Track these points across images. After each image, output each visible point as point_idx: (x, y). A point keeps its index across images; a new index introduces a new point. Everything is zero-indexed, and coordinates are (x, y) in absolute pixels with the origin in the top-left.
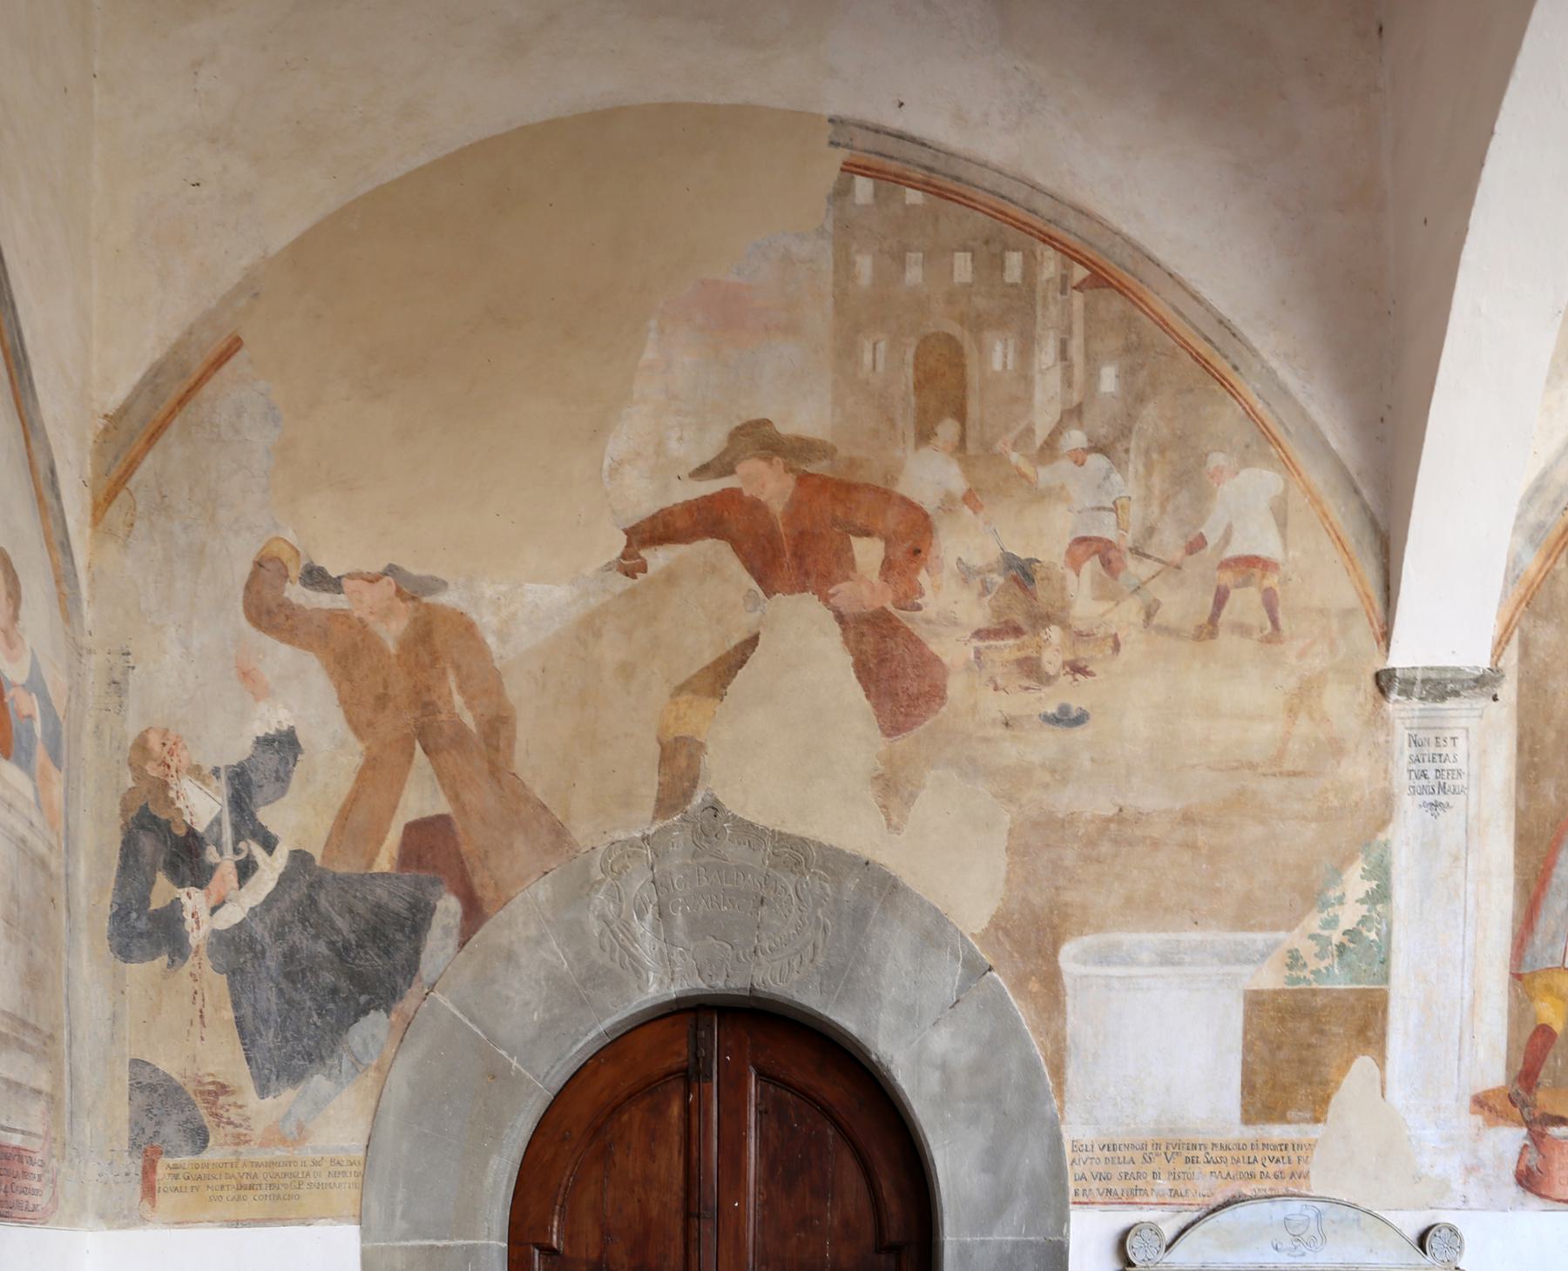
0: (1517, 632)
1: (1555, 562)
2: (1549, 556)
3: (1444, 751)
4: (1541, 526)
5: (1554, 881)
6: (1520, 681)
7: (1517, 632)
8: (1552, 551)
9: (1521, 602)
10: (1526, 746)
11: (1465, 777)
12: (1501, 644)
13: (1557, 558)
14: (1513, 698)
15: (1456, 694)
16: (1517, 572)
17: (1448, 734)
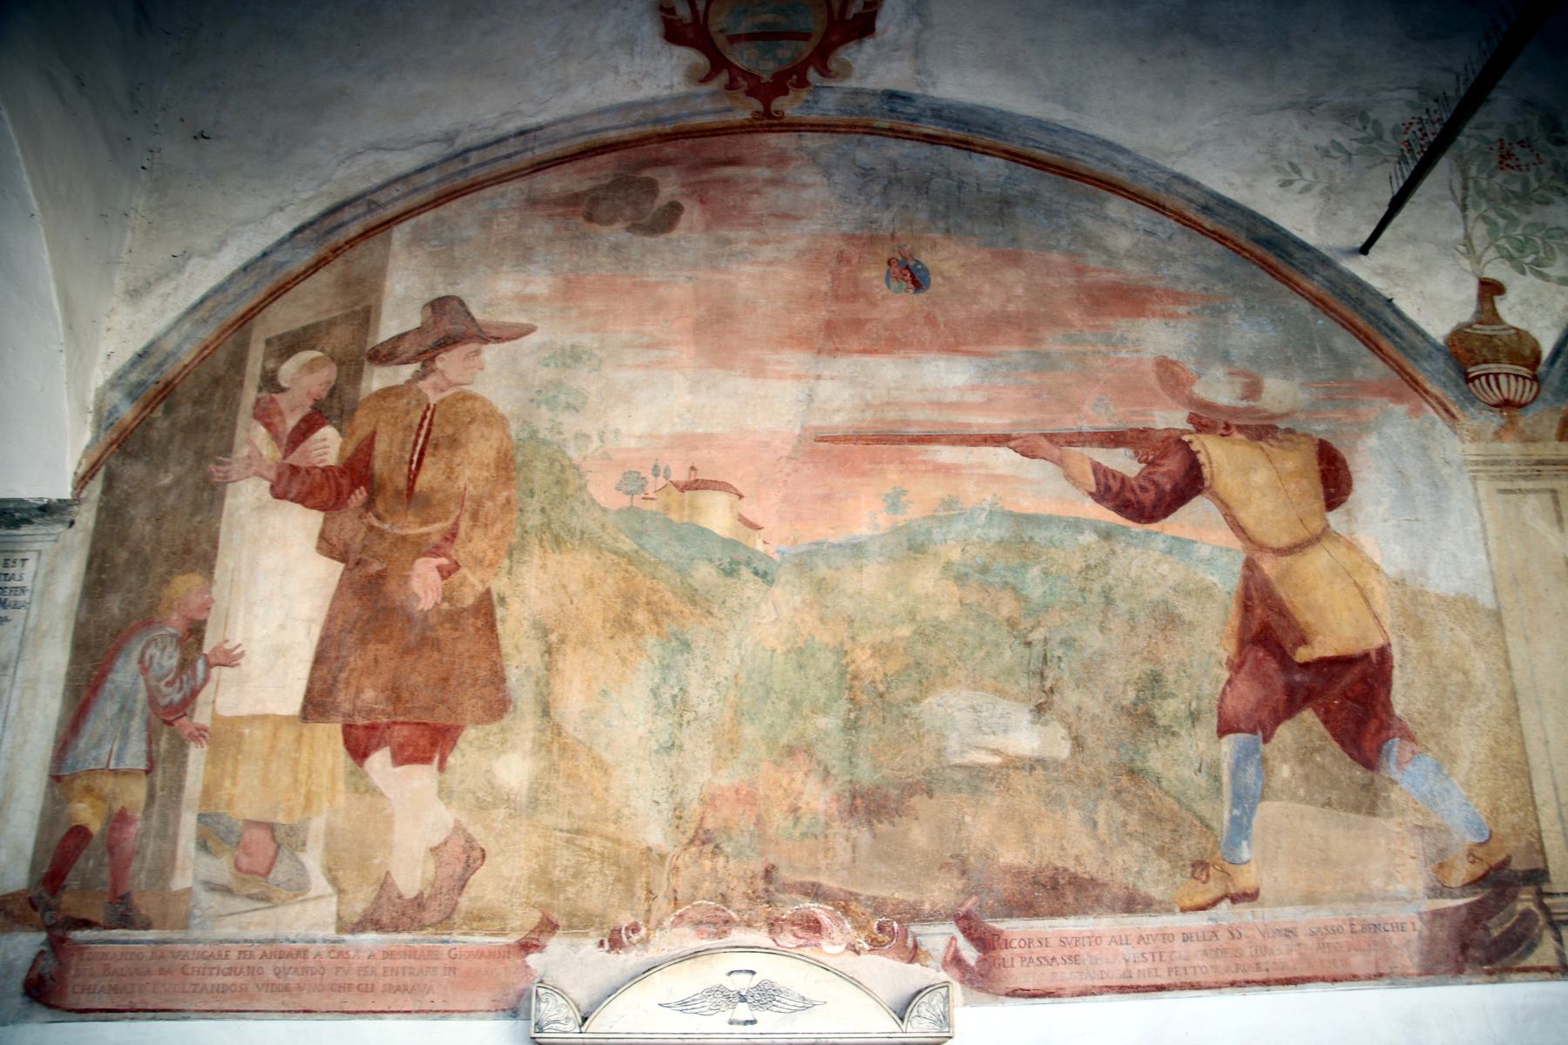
0: (103, 469)
1: (151, 412)
2: (146, 407)
3: (11, 571)
4: (141, 384)
5: (108, 686)
6: (100, 510)
7: (103, 469)
8: (150, 402)
9: (112, 444)
10: (95, 565)
11: (28, 594)
12: (82, 481)
13: (154, 408)
14: (91, 524)
15: (29, 522)
16: (111, 420)
17: (19, 556)
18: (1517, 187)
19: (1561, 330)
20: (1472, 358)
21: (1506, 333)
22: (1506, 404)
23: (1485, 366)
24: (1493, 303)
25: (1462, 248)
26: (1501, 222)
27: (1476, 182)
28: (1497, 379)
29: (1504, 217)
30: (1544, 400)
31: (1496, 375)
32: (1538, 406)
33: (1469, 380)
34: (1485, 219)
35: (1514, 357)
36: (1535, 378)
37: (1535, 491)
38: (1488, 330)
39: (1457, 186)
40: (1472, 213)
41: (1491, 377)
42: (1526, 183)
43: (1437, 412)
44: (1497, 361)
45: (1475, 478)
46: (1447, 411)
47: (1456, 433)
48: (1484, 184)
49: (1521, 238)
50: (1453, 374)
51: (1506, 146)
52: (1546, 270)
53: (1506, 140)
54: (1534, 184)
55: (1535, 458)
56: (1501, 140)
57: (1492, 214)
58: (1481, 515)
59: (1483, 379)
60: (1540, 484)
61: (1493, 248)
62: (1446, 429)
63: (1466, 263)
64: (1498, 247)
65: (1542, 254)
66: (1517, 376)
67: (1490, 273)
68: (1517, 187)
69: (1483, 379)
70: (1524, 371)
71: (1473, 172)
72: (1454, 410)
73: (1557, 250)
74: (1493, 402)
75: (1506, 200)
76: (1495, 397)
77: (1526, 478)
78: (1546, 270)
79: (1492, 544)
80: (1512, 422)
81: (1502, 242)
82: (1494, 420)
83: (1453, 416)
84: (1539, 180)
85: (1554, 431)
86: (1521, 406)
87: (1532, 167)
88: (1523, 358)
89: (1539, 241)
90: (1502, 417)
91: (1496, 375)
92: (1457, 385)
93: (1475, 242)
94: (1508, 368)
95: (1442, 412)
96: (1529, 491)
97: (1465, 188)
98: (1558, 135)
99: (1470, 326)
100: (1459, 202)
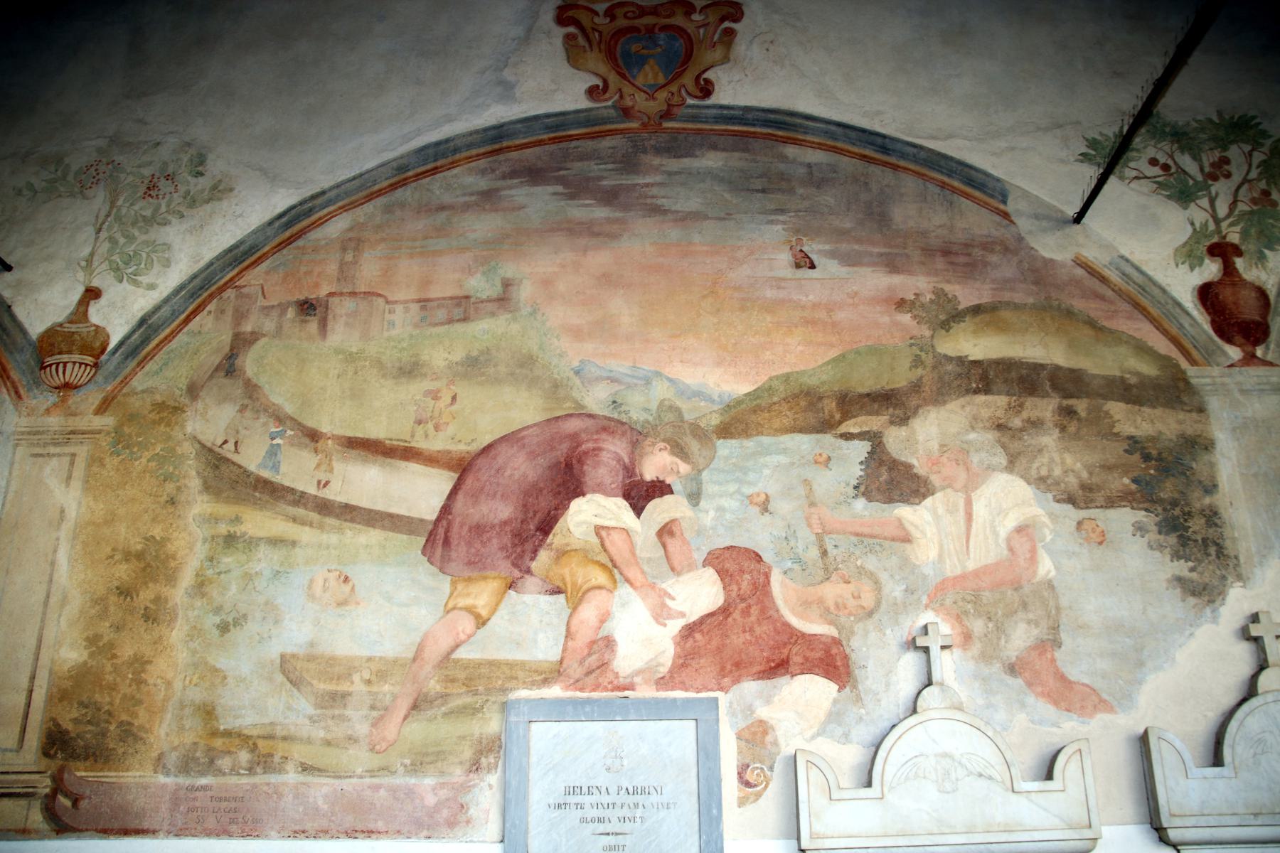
18: (148, 213)
19: (130, 326)
20: (51, 350)
21: (87, 329)
22: (67, 386)
23: (59, 356)
24: (88, 305)
25: (83, 264)
26: (122, 241)
27: (119, 210)
28: (65, 367)
29: (126, 237)
30: (96, 382)
31: (65, 364)
32: (91, 386)
33: (43, 368)
34: (112, 240)
35: (85, 349)
36: (96, 365)
37: (59, 455)
38: (73, 328)
39: (103, 214)
40: (103, 235)
41: (61, 365)
42: (157, 209)
43: (9, 395)
44: (70, 352)
45: (17, 445)
46: (17, 392)
47: (17, 410)
48: (124, 211)
49: (131, 253)
50: (33, 363)
51: (156, 180)
52: (139, 278)
53: (157, 174)
54: (163, 209)
55: (70, 429)
56: (153, 175)
57: (118, 236)
58: (10, 473)
59: (54, 367)
60: (67, 450)
61: (107, 262)
62: (11, 407)
63: (81, 275)
64: (110, 262)
65: (142, 266)
66: (81, 364)
67: (96, 283)
68: (148, 213)
69: (54, 367)
70: (89, 360)
71: (120, 203)
72: (22, 392)
73: (155, 262)
74: (55, 385)
75: (134, 224)
76: (59, 381)
77: (56, 444)
78: (139, 278)
79: (10, 496)
80: (64, 400)
81: (116, 258)
82: (53, 398)
83: (19, 397)
84: (168, 206)
85: (94, 407)
86: (76, 387)
87: (168, 196)
88: (93, 349)
89: (144, 255)
90: (59, 396)
91: (65, 364)
92: (33, 372)
93: (96, 258)
94: (77, 357)
95: (13, 394)
96: (54, 455)
97: (108, 216)
98: (200, 169)
99: (61, 325)
100: (98, 226)
